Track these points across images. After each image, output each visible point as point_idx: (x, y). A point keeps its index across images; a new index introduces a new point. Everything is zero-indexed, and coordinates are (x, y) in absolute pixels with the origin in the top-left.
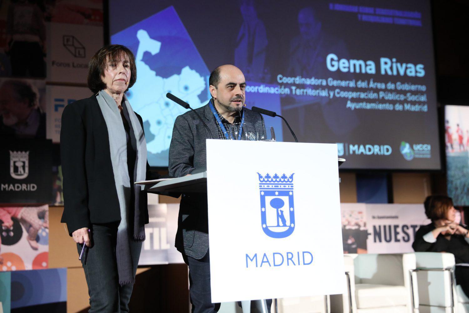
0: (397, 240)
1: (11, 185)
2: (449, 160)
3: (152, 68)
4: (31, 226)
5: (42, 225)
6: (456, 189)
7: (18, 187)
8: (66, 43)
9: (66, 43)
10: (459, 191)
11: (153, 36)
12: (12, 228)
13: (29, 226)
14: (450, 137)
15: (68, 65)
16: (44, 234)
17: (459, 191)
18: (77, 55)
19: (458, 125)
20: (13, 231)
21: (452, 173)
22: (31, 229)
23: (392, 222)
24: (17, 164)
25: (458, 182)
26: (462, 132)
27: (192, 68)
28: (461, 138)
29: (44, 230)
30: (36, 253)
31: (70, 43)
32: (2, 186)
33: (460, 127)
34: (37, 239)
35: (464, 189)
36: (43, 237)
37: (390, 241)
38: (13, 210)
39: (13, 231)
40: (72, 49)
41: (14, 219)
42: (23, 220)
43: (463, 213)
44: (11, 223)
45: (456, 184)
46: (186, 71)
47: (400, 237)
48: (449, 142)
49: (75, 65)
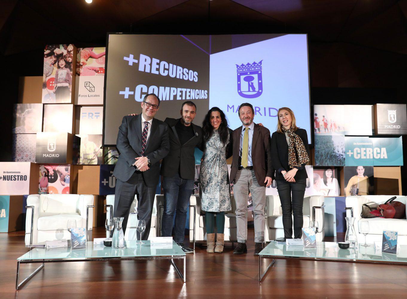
1: (48, 155)
2: (316, 138)
4: (62, 174)
5: (67, 174)
6: (322, 156)
7: (51, 156)
8: (86, 86)
9: (86, 86)
12: (53, 175)
14: (318, 124)
15: (86, 96)
18: (91, 91)
19: (324, 117)
20: (53, 176)
21: (317, 146)
22: (62, 175)
26: (326, 121)
28: (326, 124)
29: (67, 176)
31: (88, 85)
32: (44, 155)
33: (325, 118)
34: (64, 180)
35: (327, 156)
36: (67, 179)
38: (54, 167)
39: (53, 176)
40: (88, 88)
41: (54, 170)
42: (58, 171)
43: (334, 171)
44: (53, 172)
48: (316, 127)
49: (89, 96)
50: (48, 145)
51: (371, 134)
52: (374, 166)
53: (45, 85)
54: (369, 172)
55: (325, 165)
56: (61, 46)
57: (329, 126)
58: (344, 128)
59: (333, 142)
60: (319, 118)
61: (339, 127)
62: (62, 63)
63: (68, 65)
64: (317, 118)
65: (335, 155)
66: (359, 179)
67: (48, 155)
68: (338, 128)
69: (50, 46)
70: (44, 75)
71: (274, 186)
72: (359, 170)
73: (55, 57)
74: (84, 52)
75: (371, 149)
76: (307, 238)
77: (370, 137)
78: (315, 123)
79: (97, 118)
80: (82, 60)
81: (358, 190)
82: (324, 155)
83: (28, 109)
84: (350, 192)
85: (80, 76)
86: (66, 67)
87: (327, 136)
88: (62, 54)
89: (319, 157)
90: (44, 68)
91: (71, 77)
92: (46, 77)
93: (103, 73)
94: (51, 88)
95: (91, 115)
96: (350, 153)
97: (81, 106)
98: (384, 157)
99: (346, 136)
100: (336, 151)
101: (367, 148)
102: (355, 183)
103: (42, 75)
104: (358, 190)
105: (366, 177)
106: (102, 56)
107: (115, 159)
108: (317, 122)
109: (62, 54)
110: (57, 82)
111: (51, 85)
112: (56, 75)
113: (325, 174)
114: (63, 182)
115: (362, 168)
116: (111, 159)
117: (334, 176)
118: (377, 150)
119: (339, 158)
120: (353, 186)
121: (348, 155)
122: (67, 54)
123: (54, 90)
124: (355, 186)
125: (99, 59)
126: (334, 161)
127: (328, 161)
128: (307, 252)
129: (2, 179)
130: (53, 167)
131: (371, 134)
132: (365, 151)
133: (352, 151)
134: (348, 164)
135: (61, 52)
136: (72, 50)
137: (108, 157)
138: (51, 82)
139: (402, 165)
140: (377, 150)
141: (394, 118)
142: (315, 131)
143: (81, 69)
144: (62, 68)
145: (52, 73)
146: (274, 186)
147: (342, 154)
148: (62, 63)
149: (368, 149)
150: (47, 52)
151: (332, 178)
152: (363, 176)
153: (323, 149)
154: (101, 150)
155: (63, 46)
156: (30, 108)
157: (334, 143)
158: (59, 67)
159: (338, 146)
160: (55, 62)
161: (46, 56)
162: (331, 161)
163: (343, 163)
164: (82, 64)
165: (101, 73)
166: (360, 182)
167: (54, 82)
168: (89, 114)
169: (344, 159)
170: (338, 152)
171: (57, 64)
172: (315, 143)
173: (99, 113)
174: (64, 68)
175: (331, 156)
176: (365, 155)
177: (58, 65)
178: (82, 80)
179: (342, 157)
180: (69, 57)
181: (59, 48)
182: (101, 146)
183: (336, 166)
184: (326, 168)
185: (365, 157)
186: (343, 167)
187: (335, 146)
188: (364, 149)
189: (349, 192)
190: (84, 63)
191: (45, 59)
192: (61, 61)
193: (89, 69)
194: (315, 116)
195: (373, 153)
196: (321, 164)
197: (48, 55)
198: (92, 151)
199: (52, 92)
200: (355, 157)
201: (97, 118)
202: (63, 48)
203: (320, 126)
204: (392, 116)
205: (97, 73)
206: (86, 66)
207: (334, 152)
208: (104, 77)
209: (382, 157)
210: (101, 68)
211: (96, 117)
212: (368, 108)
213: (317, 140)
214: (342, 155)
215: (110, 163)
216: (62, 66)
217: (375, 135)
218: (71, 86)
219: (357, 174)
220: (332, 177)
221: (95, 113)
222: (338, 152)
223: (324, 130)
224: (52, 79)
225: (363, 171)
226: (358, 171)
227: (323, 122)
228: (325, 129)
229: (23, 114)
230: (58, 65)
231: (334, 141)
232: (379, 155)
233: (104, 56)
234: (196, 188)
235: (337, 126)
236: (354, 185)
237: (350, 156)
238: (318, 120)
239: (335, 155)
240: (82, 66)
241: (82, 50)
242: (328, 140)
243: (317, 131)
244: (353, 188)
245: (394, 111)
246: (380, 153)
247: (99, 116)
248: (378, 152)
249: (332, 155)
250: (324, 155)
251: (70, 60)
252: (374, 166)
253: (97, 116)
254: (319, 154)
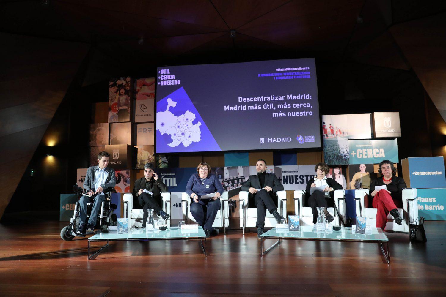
0: (296, 183)
2: (325, 143)
3: (172, 113)
4: (124, 177)
6: (330, 156)
7: (115, 163)
10: (331, 158)
11: (173, 100)
13: (123, 176)
14: (326, 131)
15: (141, 115)
16: (128, 180)
17: (331, 158)
18: (145, 111)
19: (330, 124)
21: (326, 149)
23: (294, 174)
24: (115, 154)
25: (331, 153)
26: (333, 128)
27: (190, 111)
28: (332, 131)
29: (128, 178)
30: (126, 187)
33: (332, 125)
34: (126, 181)
35: (334, 157)
37: (292, 183)
40: (143, 109)
41: (118, 174)
42: (121, 174)
43: (341, 169)
44: (118, 175)
45: (330, 154)
46: (188, 112)
47: (298, 181)
48: (325, 133)
49: (144, 115)
50: (113, 154)
51: (371, 138)
52: (374, 164)
53: (110, 109)
54: (369, 168)
55: (333, 164)
56: (121, 78)
57: (335, 132)
58: (347, 133)
59: (339, 145)
60: (326, 126)
61: (343, 133)
62: (123, 91)
63: (127, 92)
64: (325, 126)
65: (341, 156)
66: (361, 175)
67: (113, 163)
68: (342, 134)
69: (114, 79)
70: (110, 102)
71: (291, 182)
72: (362, 167)
73: (117, 87)
74: (139, 81)
75: (371, 150)
76: (291, 224)
77: (370, 139)
78: (323, 130)
79: (150, 132)
80: (138, 88)
81: (361, 184)
82: (332, 156)
83: (98, 127)
84: (355, 186)
85: (136, 101)
86: (125, 94)
87: (334, 140)
88: (123, 84)
89: (327, 158)
90: (110, 96)
91: (129, 101)
92: (111, 102)
93: (153, 97)
94: (115, 111)
95: (145, 130)
96: (353, 154)
97: (138, 123)
98: (382, 156)
99: (349, 140)
100: (341, 152)
101: (367, 149)
102: (358, 178)
103: (108, 101)
104: (361, 184)
105: (368, 173)
106: (153, 83)
107: (164, 164)
108: (324, 129)
109: (123, 84)
110: (119, 106)
111: (114, 108)
112: (118, 100)
113: (333, 172)
114: (125, 182)
115: (364, 165)
116: (161, 164)
117: (341, 173)
118: (376, 151)
119: (344, 158)
120: (357, 181)
121: (352, 155)
122: (126, 84)
123: (117, 112)
124: (359, 181)
125: (150, 86)
126: (340, 160)
127: (335, 161)
128: (291, 234)
129: (81, 181)
130: (117, 171)
131: (371, 138)
132: (366, 152)
133: (355, 152)
134: (353, 162)
135: (121, 83)
136: (129, 80)
137: (159, 163)
138: (115, 106)
139: (398, 162)
140: (376, 151)
141: (389, 124)
142: (323, 136)
143: (137, 95)
144: (123, 95)
145: (115, 99)
146: (291, 182)
147: (347, 154)
148: (123, 91)
149: (368, 150)
150: (111, 83)
151: (339, 175)
152: (365, 172)
153: (331, 151)
154: (153, 157)
155: (123, 78)
156: (100, 126)
157: (340, 146)
158: (120, 95)
159: (343, 148)
160: (117, 90)
161: (110, 86)
162: (337, 160)
163: (347, 162)
164: (137, 91)
165: (152, 97)
166: (362, 177)
167: (116, 106)
168: (144, 129)
169: (349, 158)
170: (344, 153)
171: (118, 92)
172: (324, 145)
173: (151, 128)
174: (124, 95)
175: (338, 156)
176: (366, 155)
177: (120, 92)
178: (138, 103)
179: (347, 157)
180: (127, 87)
181: (120, 80)
182: (153, 154)
183: (342, 164)
184: (334, 167)
185: (366, 157)
186: (348, 165)
187: (340, 148)
188: (366, 150)
189: (354, 186)
190: (139, 90)
191: (110, 89)
192: (122, 90)
193: (142, 94)
194: (323, 125)
195: (373, 153)
196: (329, 163)
197: (113, 86)
198: (147, 158)
199: (115, 113)
200: (358, 157)
201: (150, 132)
202: (123, 80)
203: (328, 133)
204: (388, 122)
205: (148, 98)
206: (141, 92)
207: (340, 154)
208: (154, 100)
209: (380, 156)
210: (152, 93)
211: (149, 132)
212: (367, 117)
213: (326, 144)
214: (347, 156)
215: (161, 167)
216: (122, 94)
217: (374, 138)
218: (129, 108)
219: (360, 171)
220: (340, 174)
221: (149, 129)
222: (344, 153)
223: (331, 136)
224: (115, 104)
225: (365, 168)
226: (361, 168)
227: (330, 129)
228: (332, 135)
229: (95, 131)
230: (120, 92)
231: (339, 144)
232: (378, 155)
233: (154, 84)
234: (228, 185)
235: (342, 132)
236: (358, 180)
237: (354, 156)
238: (326, 128)
239: (341, 156)
240: (137, 92)
241: (137, 80)
242: (335, 143)
243: (326, 137)
244: (357, 182)
245: (389, 117)
246: (379, 153)
247: (151, 130)
248: (377, 152)
249: (339, 155)
250: (332, 156)
251: (128, 88)
252: (374, 164)
253: (150, 131)
254: (328, 155)
